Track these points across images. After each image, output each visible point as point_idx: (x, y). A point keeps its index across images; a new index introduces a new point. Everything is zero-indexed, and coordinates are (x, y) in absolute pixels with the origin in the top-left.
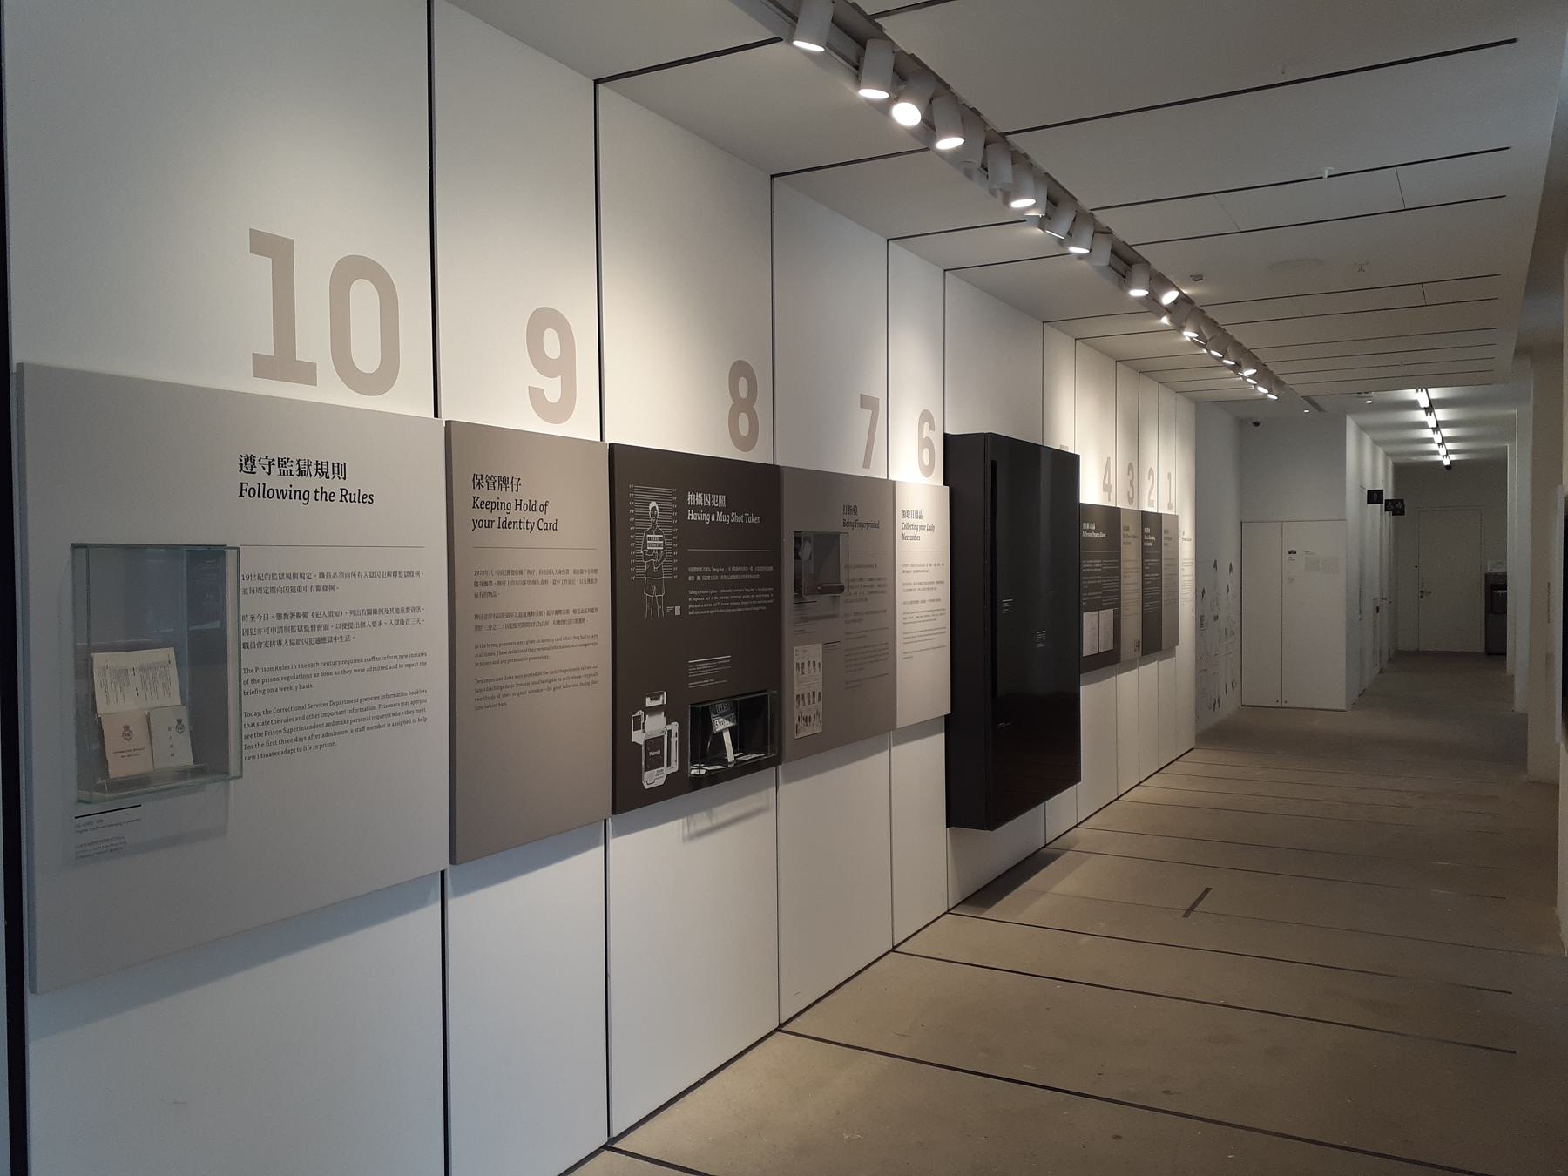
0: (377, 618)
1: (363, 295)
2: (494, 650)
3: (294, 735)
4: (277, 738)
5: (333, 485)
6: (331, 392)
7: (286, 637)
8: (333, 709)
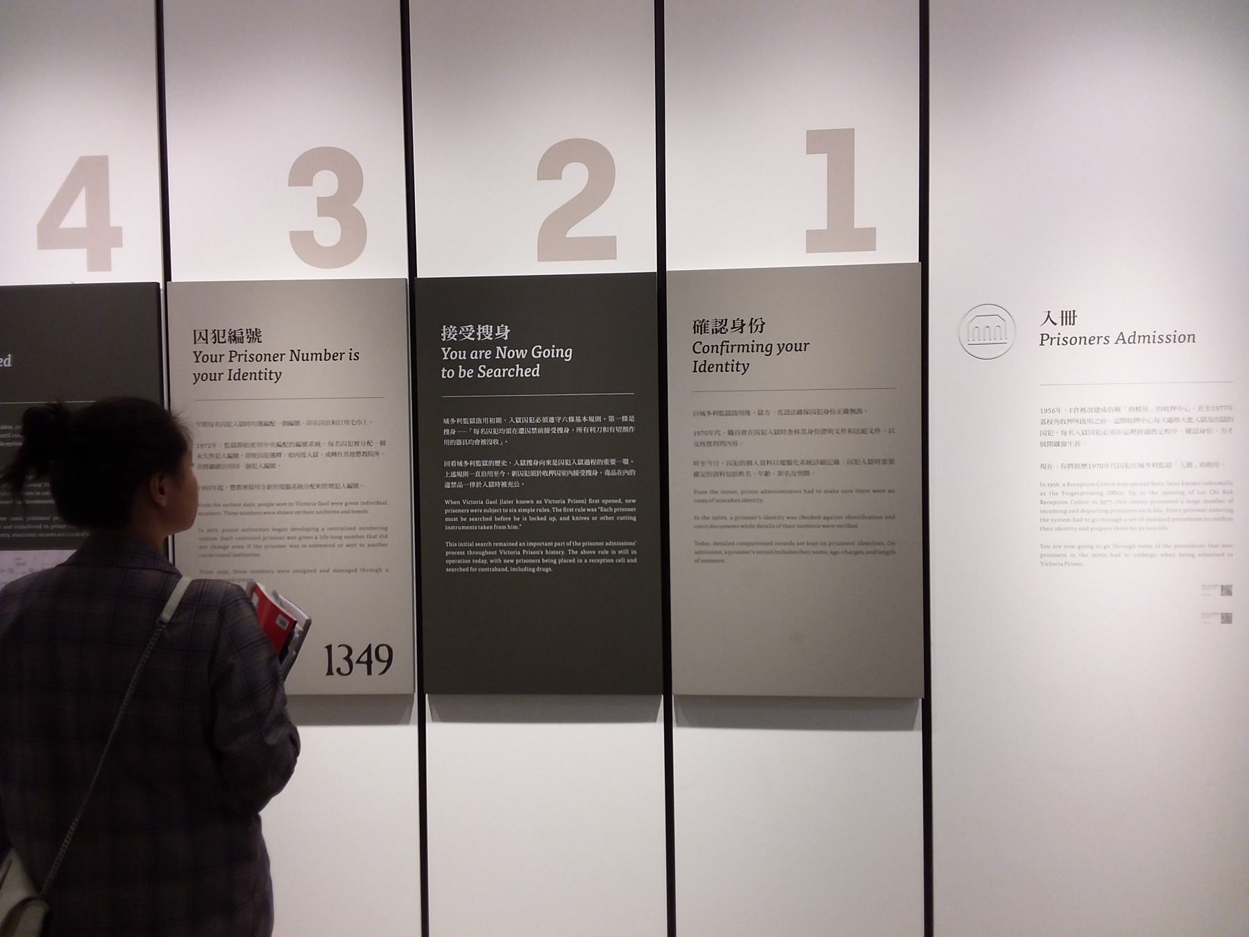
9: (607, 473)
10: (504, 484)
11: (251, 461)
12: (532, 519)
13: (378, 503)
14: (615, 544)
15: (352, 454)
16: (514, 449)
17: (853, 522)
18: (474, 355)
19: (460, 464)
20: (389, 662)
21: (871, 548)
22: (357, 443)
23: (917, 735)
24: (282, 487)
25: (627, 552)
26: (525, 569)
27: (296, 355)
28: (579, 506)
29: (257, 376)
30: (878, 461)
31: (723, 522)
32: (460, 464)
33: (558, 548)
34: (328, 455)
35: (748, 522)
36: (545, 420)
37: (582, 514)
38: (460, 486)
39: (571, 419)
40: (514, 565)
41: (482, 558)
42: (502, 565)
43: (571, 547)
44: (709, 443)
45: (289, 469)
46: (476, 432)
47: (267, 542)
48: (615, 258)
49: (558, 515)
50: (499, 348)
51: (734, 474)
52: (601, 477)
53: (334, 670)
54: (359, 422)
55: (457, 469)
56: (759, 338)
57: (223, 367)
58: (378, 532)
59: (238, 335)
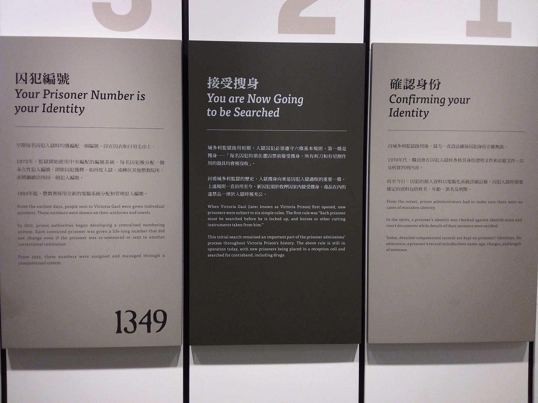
9: (326, 187)
10: (251, 194)
11: (60, 173)
12: (271, 219)
13: (157, 207)
14: (330, 237)
15: (139, 170)
16: (259, 168)
17: (494, 223)
18: (232, 100)
19: (220, 179)
20: (164, 323)
21: (506, 241)
22: (142, 162)
23: (526, 365)
24: (84, 194)
25: (338, 243)
26: (265, 255)
27: (95, 95)
28: (305, 210)
29: (65, 109)
30: (512, 182)
31: (407, 223)
32: (220, 179)
33: (289, 240)
34: (120, 170)
35: (424, 223)
36: (282, 148)
37: (308, 216)
38: (219, 195)
39: (301, 148)
40: (257, 252)
41: (235, 247)
42: (249, 252)
43: (300, 240)
44: (399, 167)
45: (90, 180)
46: (232, 156)
47: (72, 235)
48: (334, 33)
49: (290, 217)
50: (250, 95)
51: (415, 189)
52: (322, 189)
53: (122, 329)
54: (144, 147)
55: (218, 182)
56: (437, 94)
57: (39, 101)
58: (158, 228)
59: (51, 77)
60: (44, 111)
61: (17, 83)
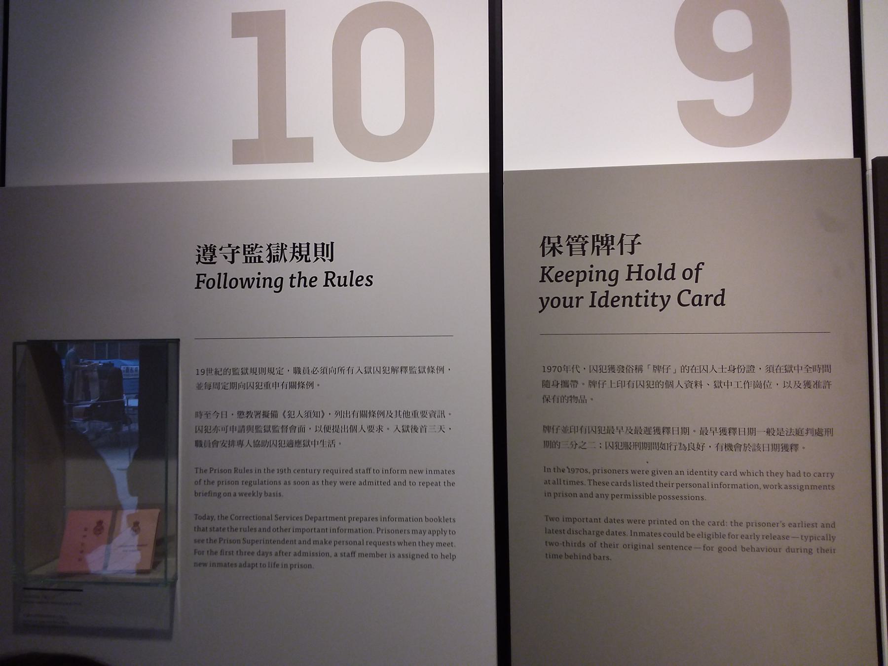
0: (375, 421)
1: (383, 50)
2: (584, 477)
3: (255, 548)
4: (235, 547)
5: (316, 268)
6: (332, 164)
7: (246, 437)
8: (310, 524)
58: (819, 531)
60: (593, 306)
61: (543, 256)
